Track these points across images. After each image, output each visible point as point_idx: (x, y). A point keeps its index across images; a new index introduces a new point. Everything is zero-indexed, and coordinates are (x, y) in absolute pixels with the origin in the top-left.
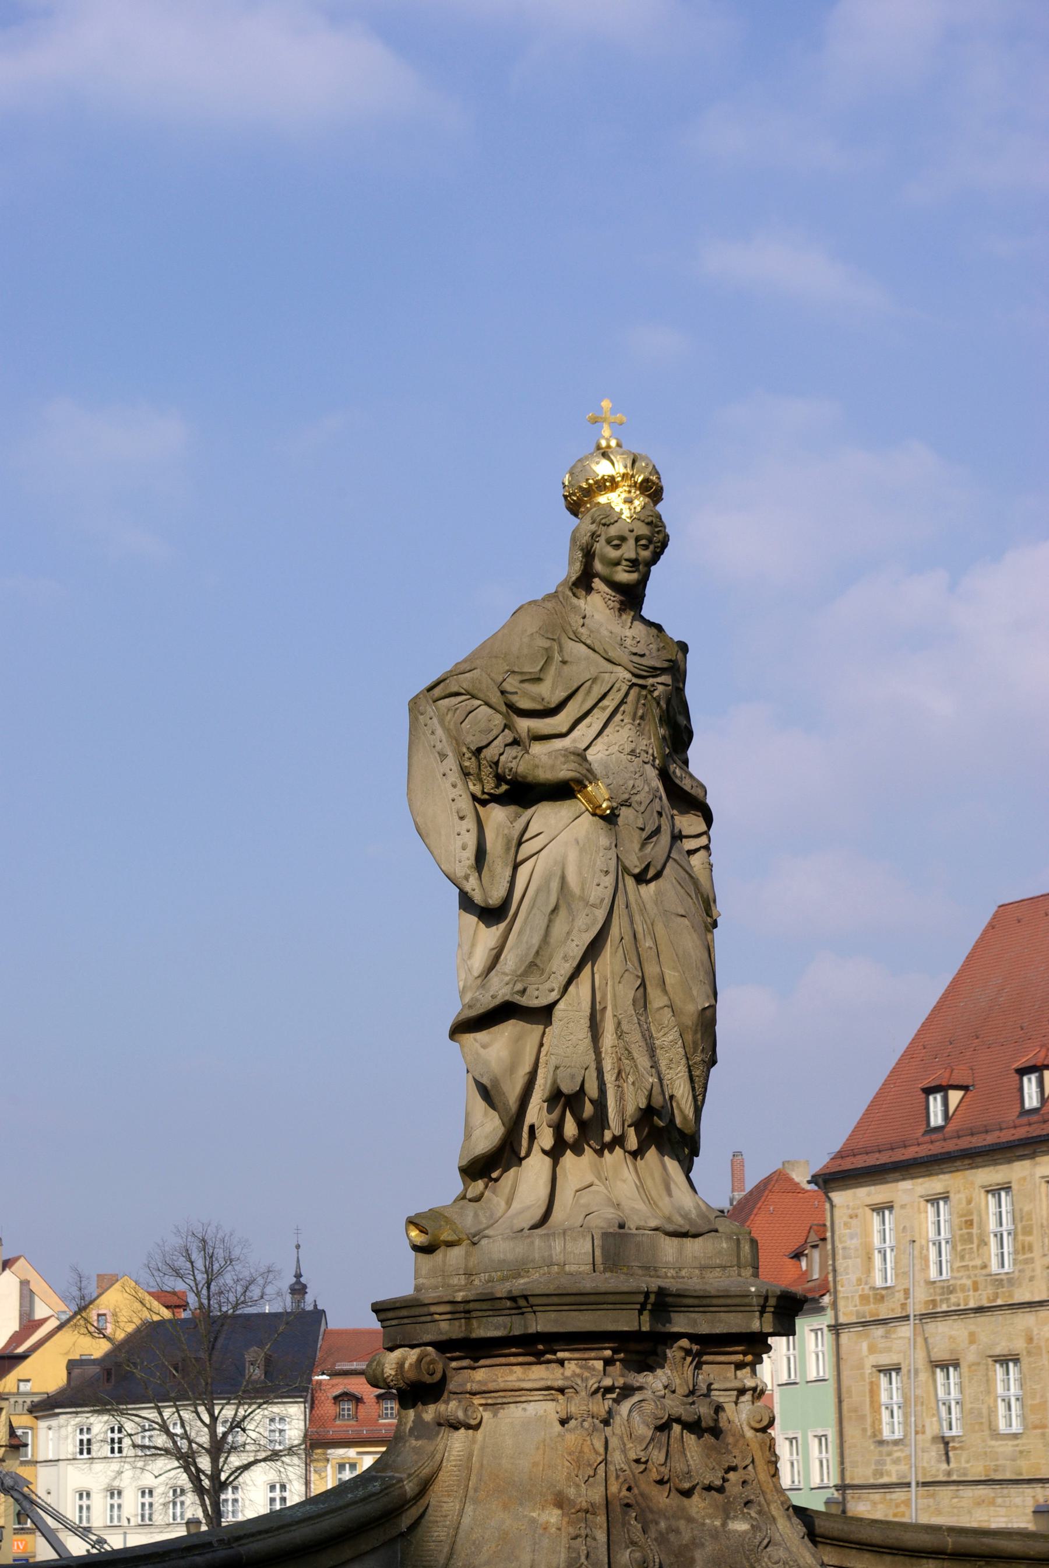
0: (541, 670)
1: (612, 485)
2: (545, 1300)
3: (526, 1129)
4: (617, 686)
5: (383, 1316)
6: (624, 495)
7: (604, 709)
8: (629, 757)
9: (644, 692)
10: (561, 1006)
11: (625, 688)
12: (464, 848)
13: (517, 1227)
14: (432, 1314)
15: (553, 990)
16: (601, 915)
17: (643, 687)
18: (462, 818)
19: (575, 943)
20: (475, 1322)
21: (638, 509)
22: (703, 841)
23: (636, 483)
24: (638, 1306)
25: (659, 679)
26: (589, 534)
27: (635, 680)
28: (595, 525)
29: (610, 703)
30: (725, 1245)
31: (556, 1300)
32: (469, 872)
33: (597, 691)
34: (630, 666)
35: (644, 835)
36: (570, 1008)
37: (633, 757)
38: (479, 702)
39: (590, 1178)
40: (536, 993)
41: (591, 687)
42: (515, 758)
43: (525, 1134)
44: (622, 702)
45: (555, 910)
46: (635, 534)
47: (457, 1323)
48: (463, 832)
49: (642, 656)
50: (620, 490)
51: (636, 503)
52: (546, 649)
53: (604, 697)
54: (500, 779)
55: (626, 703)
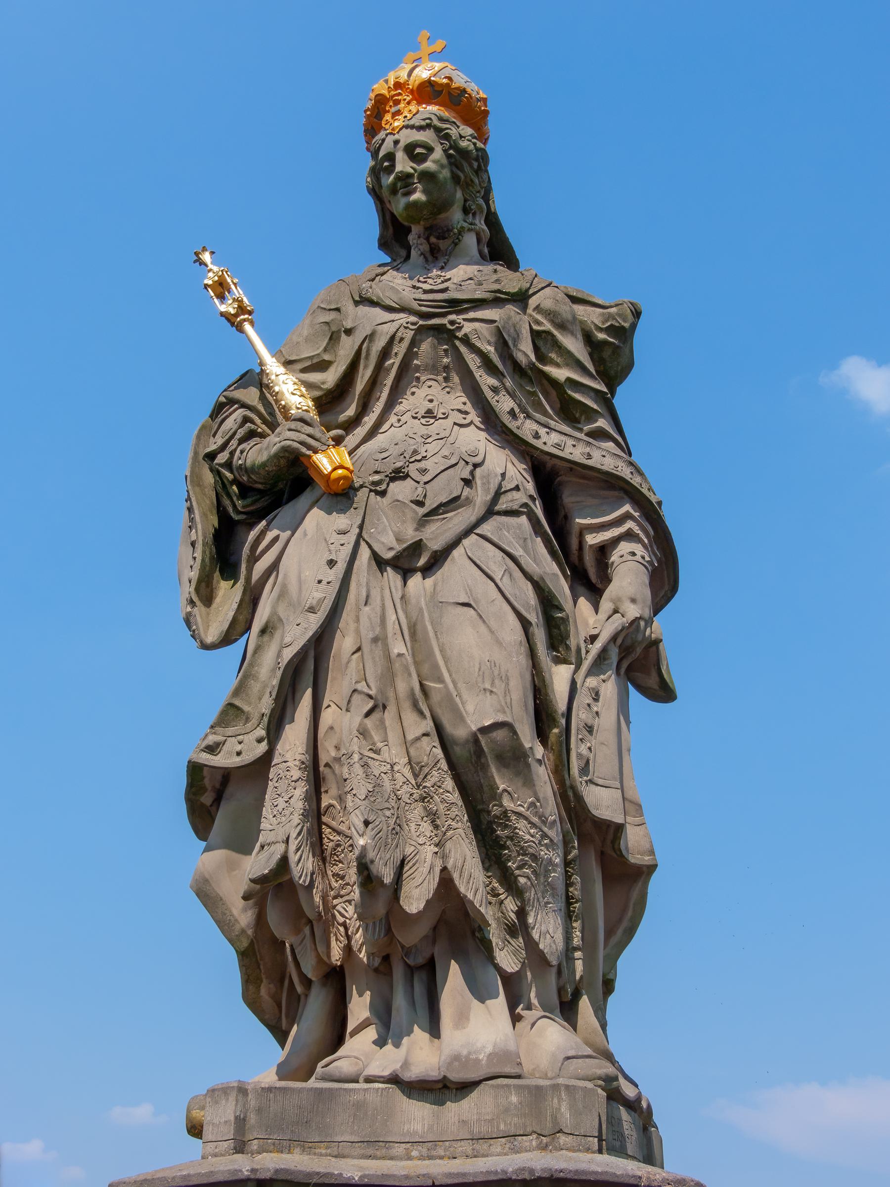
4: (399, 334)
8: (423, 421)
15: (259, 741)
16: (314, 622)
29: (394, 362)
30: (514, 1099)
34: (415, 305)
35: (422, 511)
37: (432, 421)
40: (239, 748)
44: (410, 355)
46: (402, 144)
53: (385, 353)
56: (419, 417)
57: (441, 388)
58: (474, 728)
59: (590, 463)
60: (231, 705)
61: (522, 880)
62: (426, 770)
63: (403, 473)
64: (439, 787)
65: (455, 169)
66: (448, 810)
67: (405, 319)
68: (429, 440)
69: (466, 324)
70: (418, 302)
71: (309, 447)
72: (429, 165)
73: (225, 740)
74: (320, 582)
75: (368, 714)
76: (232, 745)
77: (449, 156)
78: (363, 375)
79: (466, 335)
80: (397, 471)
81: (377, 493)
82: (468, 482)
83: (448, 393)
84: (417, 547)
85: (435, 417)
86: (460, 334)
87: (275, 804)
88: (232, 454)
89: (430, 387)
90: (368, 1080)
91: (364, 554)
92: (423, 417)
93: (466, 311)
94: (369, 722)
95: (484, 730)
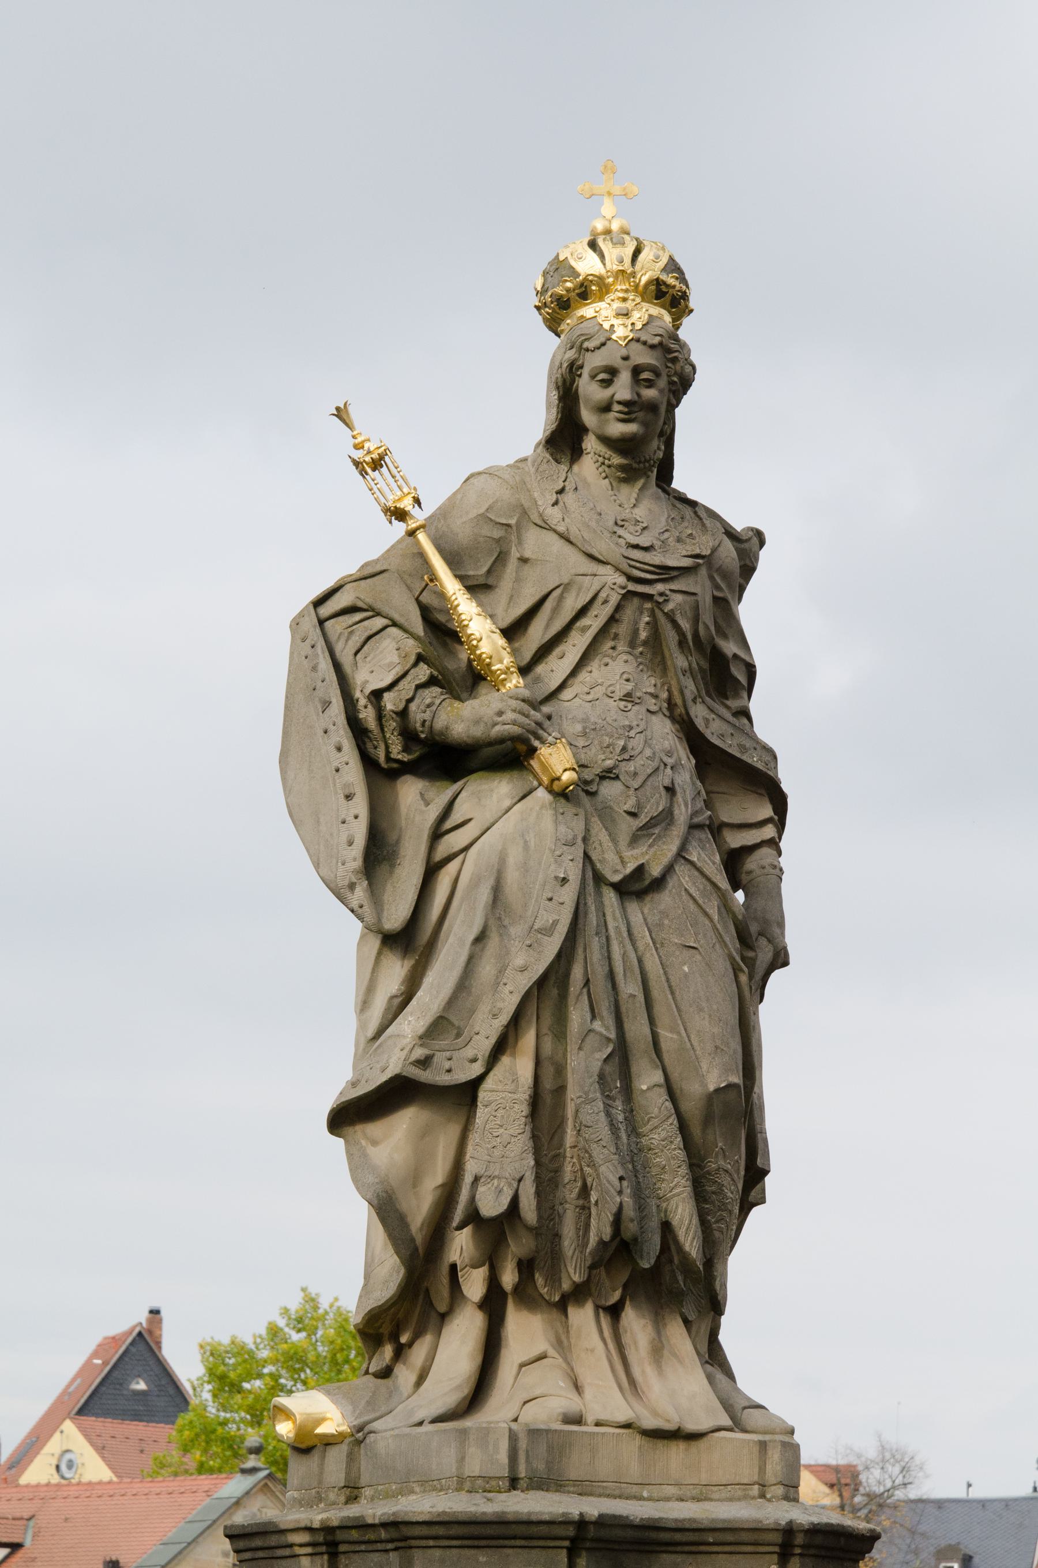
0: (489, 572)
1: (600, 290)
2: (425, 1531)
3: (445, 1270)
4: (603, 595)
5: (242, 1544)
6: (617, 305)
7: (584, 630)
8: (622, 704)
9: (648, 605)
10: (489, 1083)
11: (614, 599)
12: (350, 843)
13: (417, 1418)
14: (291, 1546)
15: (474, 1060)
16: (552, 947)
17: (648, 597)
18: (349, 797)
19: (509, 988)
20: (343, 1560)
21: (639, 326)
22: (769, 832)
23: (637, 286)
24: (567, 1543)
25: (674, 586)
26: (565, 365)
27: (632, 587)
28: (574, 350)
29: (593, 622)
31: (441, 1531)
32: (354, 880)
33: (572, 603)
34: (624, 566)
36: (500, 1088)
37: (630, 705)
38: (385, 622)
39: (542, 1345)
40: (447, 1065)
41: (561, 598)
42: (429, 706)
43: (445, 1279)
44: (612, 620)
45: (480, 939)
47: (317, 1559)
48: (351, 819)
49: (646, 549)
50: (612, 296)
51: (636, 315)
52: (498, 541)
53: (583, 612)
54: (409, 736)
55: (617, 621)
57: (636, 665)
58: (712, 1088)
59: (744, 758)
60: (441, 1017)
61: (717, 1234)
62: (654, 1122)
64: (671, 1142)
65: (671, 396)
66: (679, 1167)
67: (610, 577)
68: (632, 733)
70: (629, 561)
71: (538, 737)
72: (650, 393)
73: (433, 1055)
74: (550, 899)
75: (606, 1060)
76: (439, 1058)
77: (671, 383)
80: (609, 770)
81: (588, 793)
82: (670, 790)
84: (640, 870)
87: (495, 1134)
88: (410, 701)
89: (626, 662)
90: (598, 1424)
91: (589, 874)
92: (620, 700)
94: (608, 1069)
95: (718, 1091)
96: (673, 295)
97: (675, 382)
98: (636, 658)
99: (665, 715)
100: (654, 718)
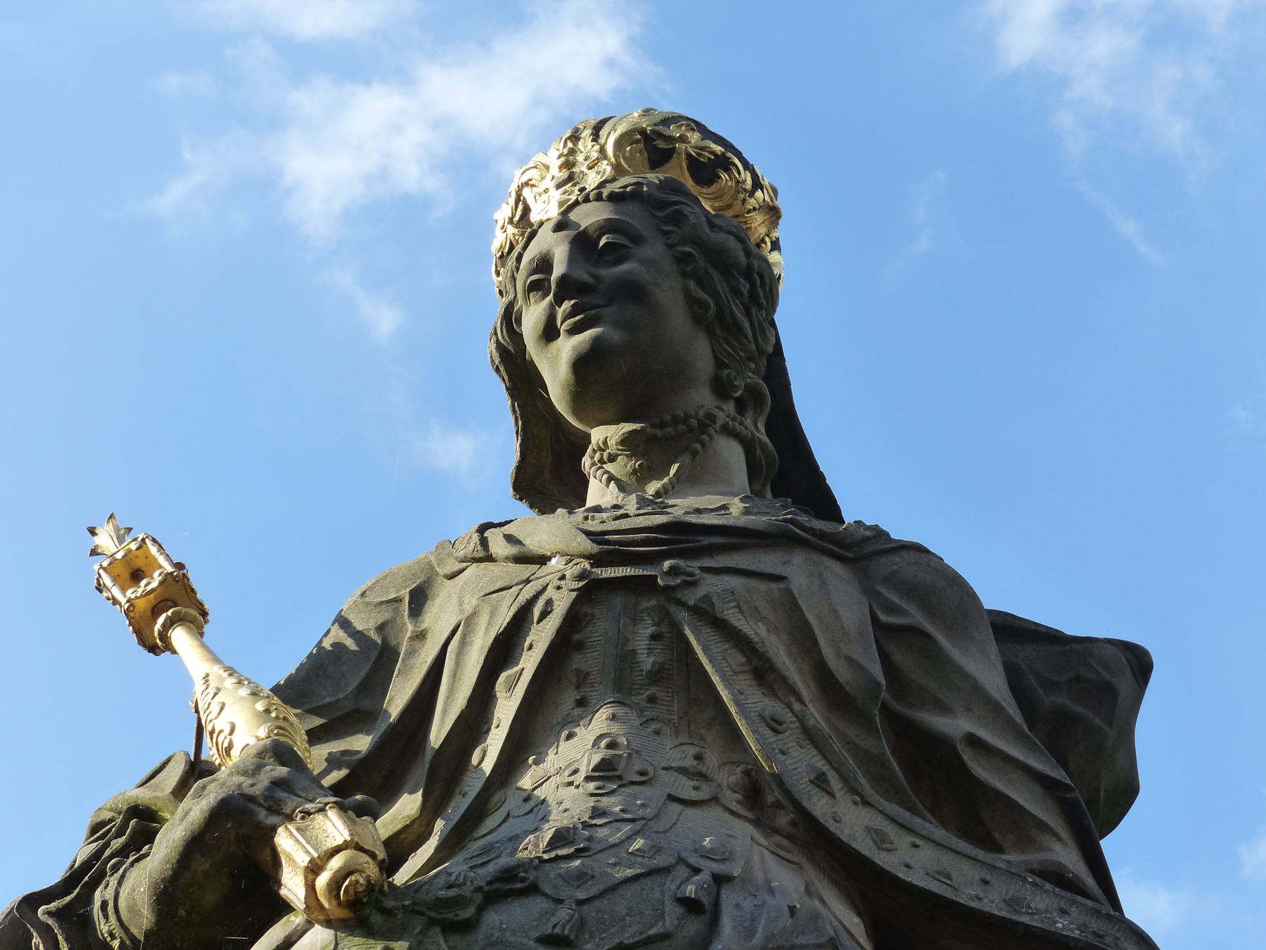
11: (562, 602)
41: (464, 643)
55: (580, 646)
56: (579, 778)
57: (638, 722)
63: (523, 880)
65: (692, 284)
69: (710, 579)
78: (445, 712)
79: (707, 598)
83: (657, 733)
85: (620, 778)
86: (692, 597)
93: (712, 550)
96: (689, 156)
97: (690, 254)
98: (641, 711)
99: (733, 813)
100: (691, 812)
